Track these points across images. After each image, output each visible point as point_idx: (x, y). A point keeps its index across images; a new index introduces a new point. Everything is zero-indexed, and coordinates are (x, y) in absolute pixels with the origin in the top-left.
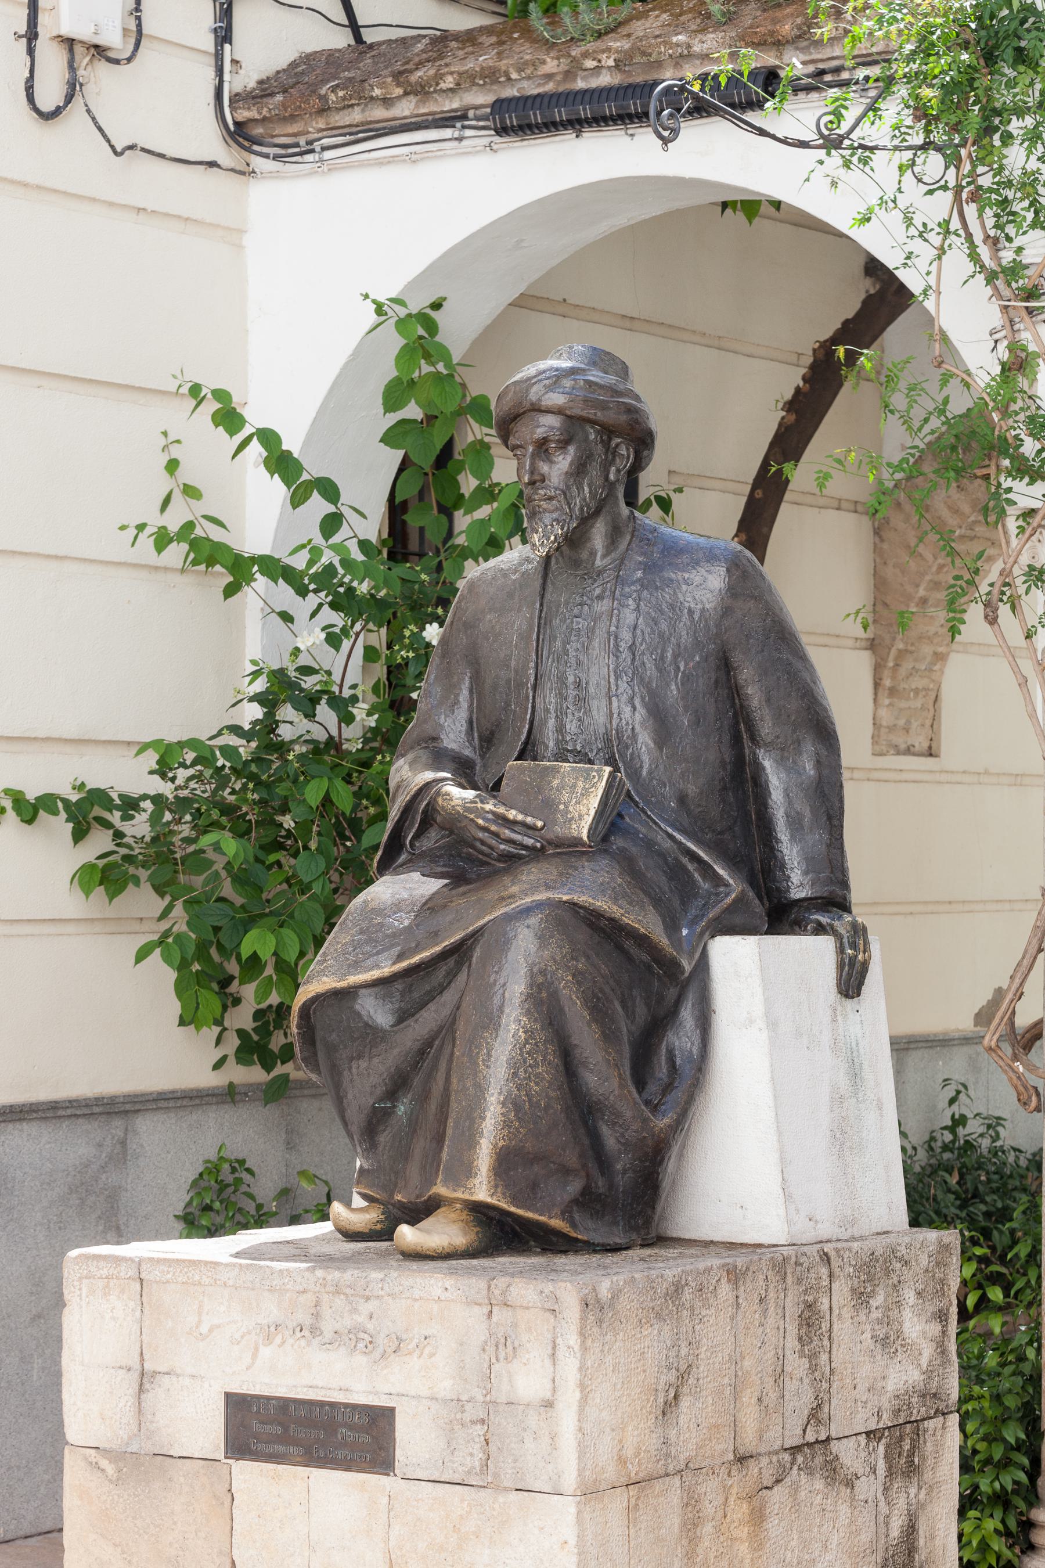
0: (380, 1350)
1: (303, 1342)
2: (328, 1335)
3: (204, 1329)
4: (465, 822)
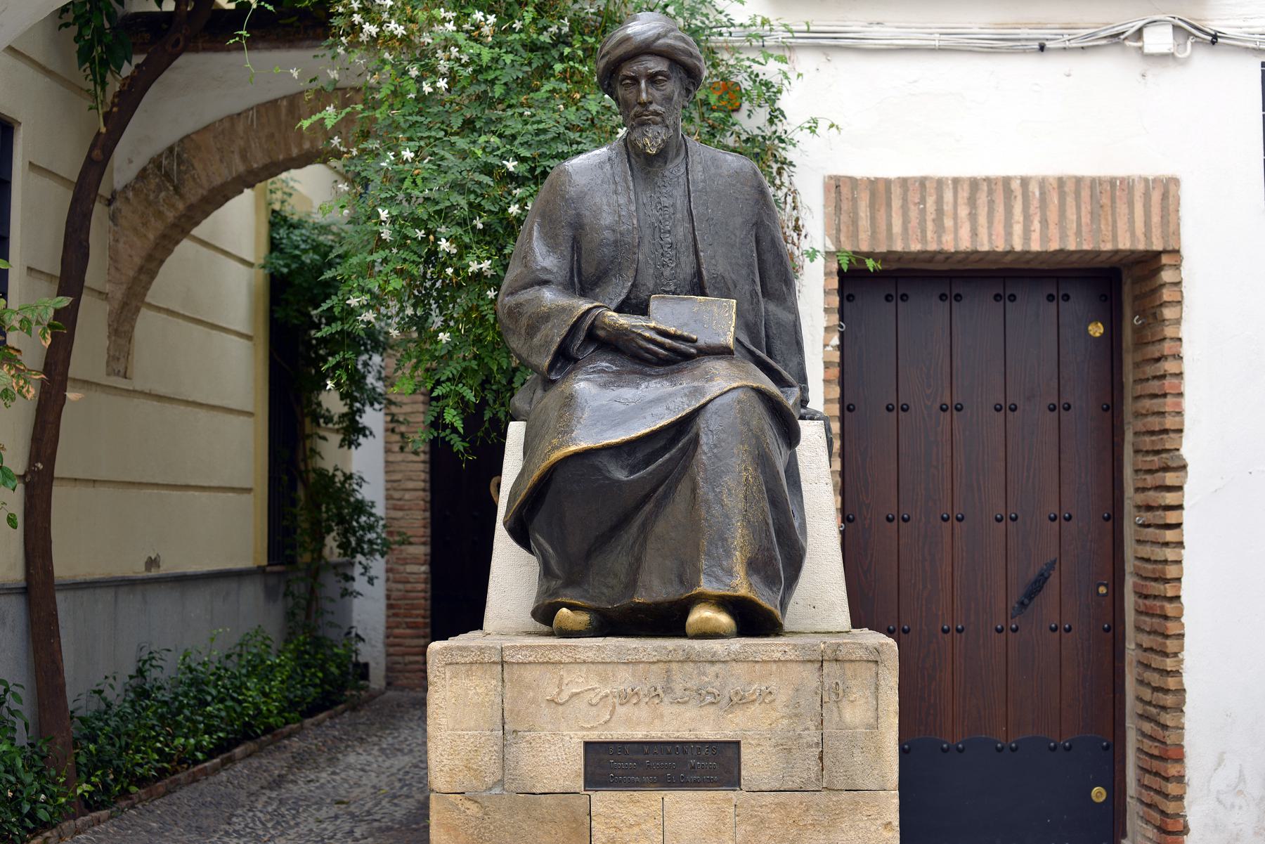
3: (564, 697)
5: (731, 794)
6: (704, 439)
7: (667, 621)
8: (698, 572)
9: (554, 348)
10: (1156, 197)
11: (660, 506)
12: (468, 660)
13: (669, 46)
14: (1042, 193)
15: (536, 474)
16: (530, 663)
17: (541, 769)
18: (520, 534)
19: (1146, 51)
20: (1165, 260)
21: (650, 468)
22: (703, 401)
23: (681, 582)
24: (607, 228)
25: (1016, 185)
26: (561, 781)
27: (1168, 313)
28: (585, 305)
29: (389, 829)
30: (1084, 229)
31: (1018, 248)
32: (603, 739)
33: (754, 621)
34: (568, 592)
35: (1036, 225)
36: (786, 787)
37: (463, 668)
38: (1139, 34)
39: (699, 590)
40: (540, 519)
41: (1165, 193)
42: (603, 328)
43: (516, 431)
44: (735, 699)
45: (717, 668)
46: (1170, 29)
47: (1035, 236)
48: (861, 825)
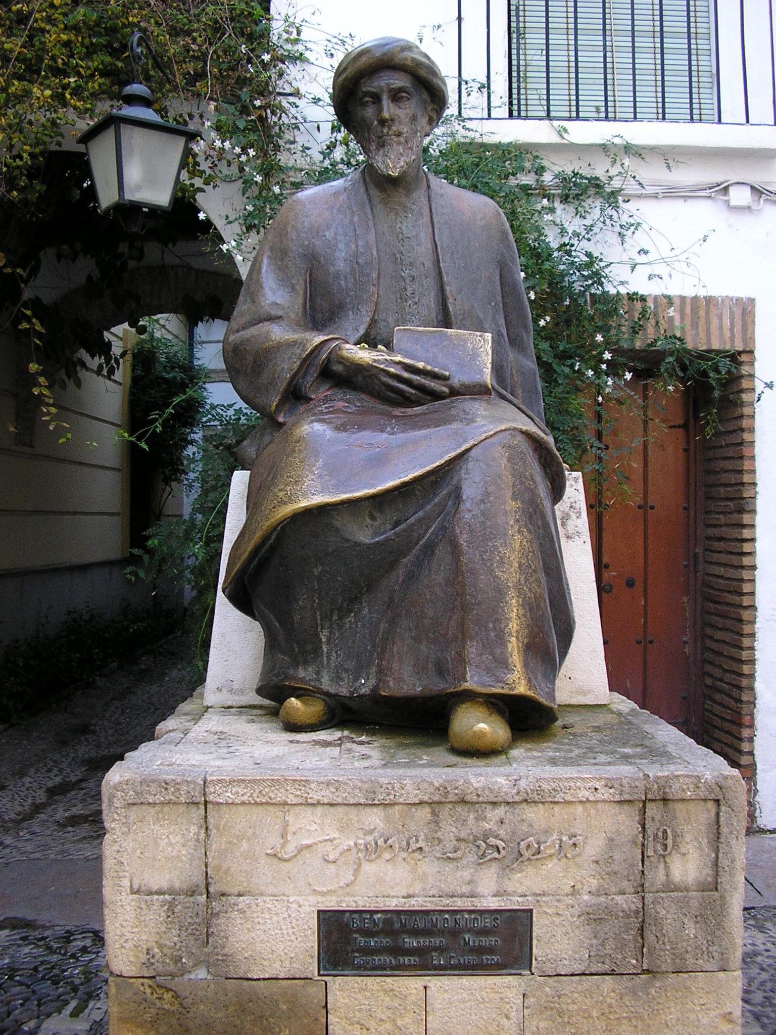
1: (417, 855)
2: (450, 845)
3: (291, 849)
4: (374, 371)
8: (461, 661)
9: (282, 386)
10: (738, 313)
13: (413, 59)
15: (259, 534)
16: (243, 803)
18: (243, 600)
19: (732, 203)
26: (287, 964)
27: (745, 397)
33: (529, 719)
36: (593, 971)
37: (152, 811)
38: (726, 190)
41: (745, 310)
42: (340, 362)
43: (240, 480)
44: (527, 854)
45: (501, 811)
46: (748, 190)
48: (692, 1017)
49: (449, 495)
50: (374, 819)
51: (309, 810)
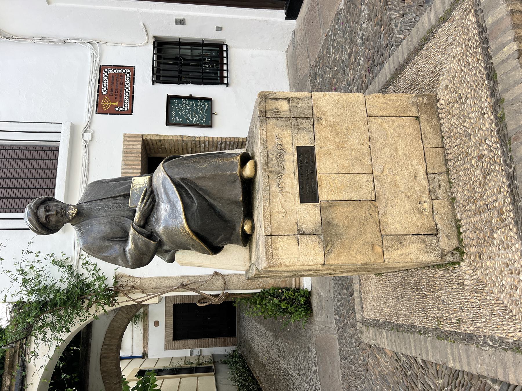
0: (281, 151)
1: (283, 176)
3: (283, 211)
4: (143, 210)
5: (316, 149)
6: (182, 176)
7: (248, 185)
10: (128, 139)
11: (206, 193)
12: (270, 249)
14: (126, 165)
17: (312, 219)
20: (144, 138)
21: (193, 196)
22: (167, 177)
23: (235, 182)
24: (105, 227)
25: (123, 171)
28: (132, 231)
29: (275, 335)
30: (136, 155)
31: (140, 171)
32: (299, 196)
34: (237, 229)
35: (134, 167)
37: (274, 251)
39: (238, 173)
40: (211, 239)
44: (282, 148)
45: (270, 155)
47: (137, 167)
49: (183, 182)
50: (274, 188)
51: (271, 206)
